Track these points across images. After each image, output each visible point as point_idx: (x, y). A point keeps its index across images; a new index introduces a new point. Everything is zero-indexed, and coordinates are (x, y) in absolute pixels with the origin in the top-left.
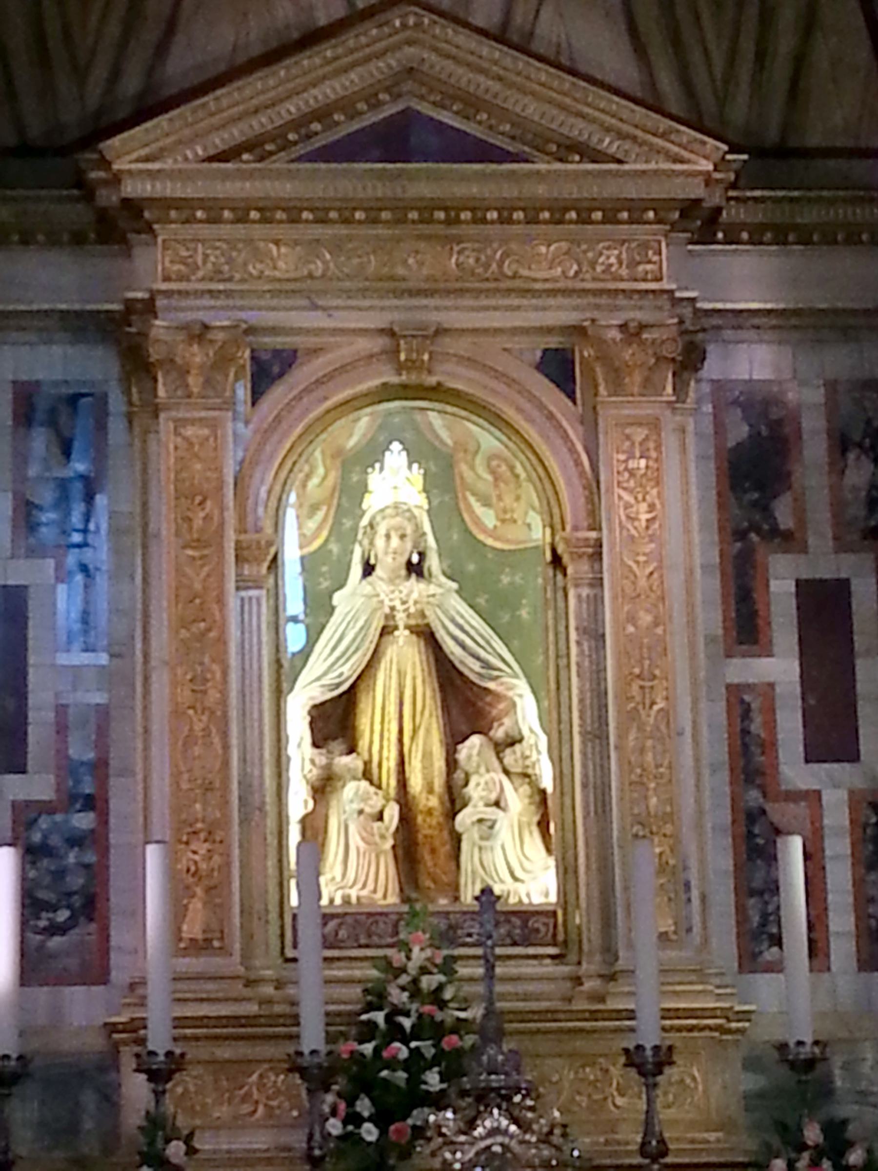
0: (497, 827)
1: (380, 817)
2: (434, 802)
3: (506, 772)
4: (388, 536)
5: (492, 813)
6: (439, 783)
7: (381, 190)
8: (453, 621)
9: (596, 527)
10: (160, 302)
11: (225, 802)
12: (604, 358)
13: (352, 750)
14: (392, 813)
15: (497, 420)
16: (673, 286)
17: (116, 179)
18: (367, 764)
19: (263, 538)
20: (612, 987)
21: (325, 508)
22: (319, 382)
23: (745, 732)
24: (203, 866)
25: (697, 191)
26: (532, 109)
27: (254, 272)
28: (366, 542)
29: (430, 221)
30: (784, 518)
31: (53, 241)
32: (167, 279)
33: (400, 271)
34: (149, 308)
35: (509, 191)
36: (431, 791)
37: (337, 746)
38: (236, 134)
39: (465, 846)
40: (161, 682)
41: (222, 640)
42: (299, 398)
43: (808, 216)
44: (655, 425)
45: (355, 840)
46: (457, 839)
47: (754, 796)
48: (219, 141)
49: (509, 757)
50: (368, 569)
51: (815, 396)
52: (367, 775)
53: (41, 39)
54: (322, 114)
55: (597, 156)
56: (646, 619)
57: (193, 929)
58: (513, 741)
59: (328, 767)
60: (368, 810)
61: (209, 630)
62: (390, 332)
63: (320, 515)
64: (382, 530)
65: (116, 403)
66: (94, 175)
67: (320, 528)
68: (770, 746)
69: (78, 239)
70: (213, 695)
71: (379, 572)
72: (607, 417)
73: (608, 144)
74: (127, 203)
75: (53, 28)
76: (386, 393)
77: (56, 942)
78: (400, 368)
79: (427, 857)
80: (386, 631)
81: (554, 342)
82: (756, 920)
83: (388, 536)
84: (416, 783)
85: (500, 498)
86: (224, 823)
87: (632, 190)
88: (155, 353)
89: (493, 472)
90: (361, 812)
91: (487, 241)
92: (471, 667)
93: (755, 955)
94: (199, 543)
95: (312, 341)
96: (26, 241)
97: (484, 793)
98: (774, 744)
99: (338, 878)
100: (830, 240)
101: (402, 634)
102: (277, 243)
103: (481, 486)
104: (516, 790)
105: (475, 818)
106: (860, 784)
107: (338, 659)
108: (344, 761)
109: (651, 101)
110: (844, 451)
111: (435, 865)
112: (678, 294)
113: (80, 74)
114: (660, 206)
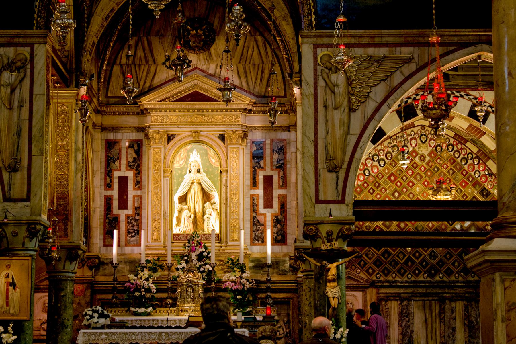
1: (190, 217)
2: (200, 214)
3: (213, 209)
5: (210, 216)
6: (201, 210)
7: (190, 107)
9: (227, 167)
10: (151, 127)
11: (160, 216)
12: (230, 137)
13: (186, 204)
14: (192, 216)
15: (211, 147)
18: (189, 207)
19: (168, 169)
20: (227, 248)
22: (179, 141)
23: (253, 203)
24: (157, 227)
25: (246, 107)
29: (199, 112)
30: (262, 164)
31: (133, 114)
32: (152, 122)
33: (194, 121)
34: (149, 127)
35: (213, 107)
36: (199, 212)
37: (184, 204)
38: (164, 97)
40: (150, 194)
41: (161, 187)
42: (176, 143)
45: (186, 221)
46: (204, 220)
47: (254, 214)
48: (161, 98)
49: (213, 206)
50: (190, 172)
51: (268, 142)
52: (188, 209)
54: (180, 92)
56: (235, 184)
57: (155, 237)
58: (214, 203)
59: (182, 207)
62: (191, 131)
64: (192, 164)
66: (140, 104)
67: (183, 163)
68: (257, 205)
69: (138, 113)
70: (159, 197)
71: (192, 172)
72: (230, 146)
74: (145, 109)
76: (191, 142)
77: (132, 239)
78: (194, 138)
80: (192, 183)
81: (221, 133)
82: (254, 236)
84: (197, 211)
86: (160, 219)
88: (150, 136)
91: (209, 115)
92: (207, 190)
93: (253, 243)
94: (158, 170)
98: (258, 205)
102: (172, 116)
106: (273, 212)
108: (185, 207)
109: (241, 87)
110: (273, 152)
114: (240, 109)
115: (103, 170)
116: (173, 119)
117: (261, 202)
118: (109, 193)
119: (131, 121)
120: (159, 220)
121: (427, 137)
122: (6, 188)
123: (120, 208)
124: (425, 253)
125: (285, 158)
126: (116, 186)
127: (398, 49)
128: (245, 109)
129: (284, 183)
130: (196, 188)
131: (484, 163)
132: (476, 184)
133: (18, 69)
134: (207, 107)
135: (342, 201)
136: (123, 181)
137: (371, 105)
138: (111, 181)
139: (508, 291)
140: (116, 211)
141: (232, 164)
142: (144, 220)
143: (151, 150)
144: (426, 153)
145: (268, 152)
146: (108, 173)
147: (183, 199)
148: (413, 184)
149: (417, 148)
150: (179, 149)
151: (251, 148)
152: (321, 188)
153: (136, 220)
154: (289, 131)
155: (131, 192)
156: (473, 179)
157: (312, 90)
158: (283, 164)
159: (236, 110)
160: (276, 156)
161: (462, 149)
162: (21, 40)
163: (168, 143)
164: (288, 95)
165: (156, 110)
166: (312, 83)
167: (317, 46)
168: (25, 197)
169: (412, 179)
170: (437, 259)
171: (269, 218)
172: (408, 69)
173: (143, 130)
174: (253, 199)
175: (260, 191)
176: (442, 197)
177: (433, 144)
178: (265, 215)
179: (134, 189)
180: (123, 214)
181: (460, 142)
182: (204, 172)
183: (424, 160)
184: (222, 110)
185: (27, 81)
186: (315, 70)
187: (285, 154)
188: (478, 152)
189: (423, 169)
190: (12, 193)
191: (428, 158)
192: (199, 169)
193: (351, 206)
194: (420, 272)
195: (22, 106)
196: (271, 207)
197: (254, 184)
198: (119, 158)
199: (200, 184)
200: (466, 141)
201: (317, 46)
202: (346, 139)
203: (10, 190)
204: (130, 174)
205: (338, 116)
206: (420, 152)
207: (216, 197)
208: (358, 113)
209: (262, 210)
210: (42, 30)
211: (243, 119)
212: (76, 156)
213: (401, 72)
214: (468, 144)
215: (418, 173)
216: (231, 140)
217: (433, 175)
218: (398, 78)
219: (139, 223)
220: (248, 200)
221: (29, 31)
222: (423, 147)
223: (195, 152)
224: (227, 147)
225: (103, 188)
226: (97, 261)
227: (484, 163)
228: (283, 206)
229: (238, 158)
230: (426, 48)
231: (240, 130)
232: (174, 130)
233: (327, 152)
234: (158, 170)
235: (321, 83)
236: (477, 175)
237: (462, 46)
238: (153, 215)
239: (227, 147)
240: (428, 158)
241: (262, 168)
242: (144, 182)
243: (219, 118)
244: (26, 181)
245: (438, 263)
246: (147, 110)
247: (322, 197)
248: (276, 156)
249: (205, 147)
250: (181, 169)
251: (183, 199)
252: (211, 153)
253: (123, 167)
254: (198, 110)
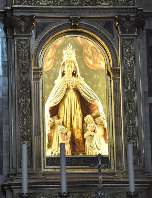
0: (94, 137)
1: (66, 134)
2: (79, 131)
3: (96, 124)
4: (68, 67)
5: (93, 133)
6: (80, 126)
8: (83, 87)
11: (31, 131)
13: (59, 118)
14: (69, 133)
16: (137, 7)
21: (52, 59)
27: (37, 3)
28: (62, 68)
37: (56, 117)
39: (86, 141)
46: (84, 140)
49: (97, 120)
50: (63, 75)
52: (63, 124)
58: (98, 116)
59: (54, 122)
60: (63, 132)
61: (26, 90)
63: (51, 61)
64: (66, 65)
71: (65, 75)
79: (77, 144)
80: (68, 90)
81: (108, 20)
83: (68, 67)
84: (75, 126)
85: (94, 57)
86: (31, 136)
89: (92, 51)
90: (62, 133)
92: (87, 98)
95: (50, 20)
97: (91, 129)
99: (57, 149)
101: (71, 91)
103: (89, 54)
104: (98, 128)
105: (89, 135)
107: (56, 97)
111: (79, 145)
112: (138, 9)
130: (72, 96)
147: (55, 111)
192: (76, 71)
199: (77, 91)
223: (70, 47)
251: (55, 111)
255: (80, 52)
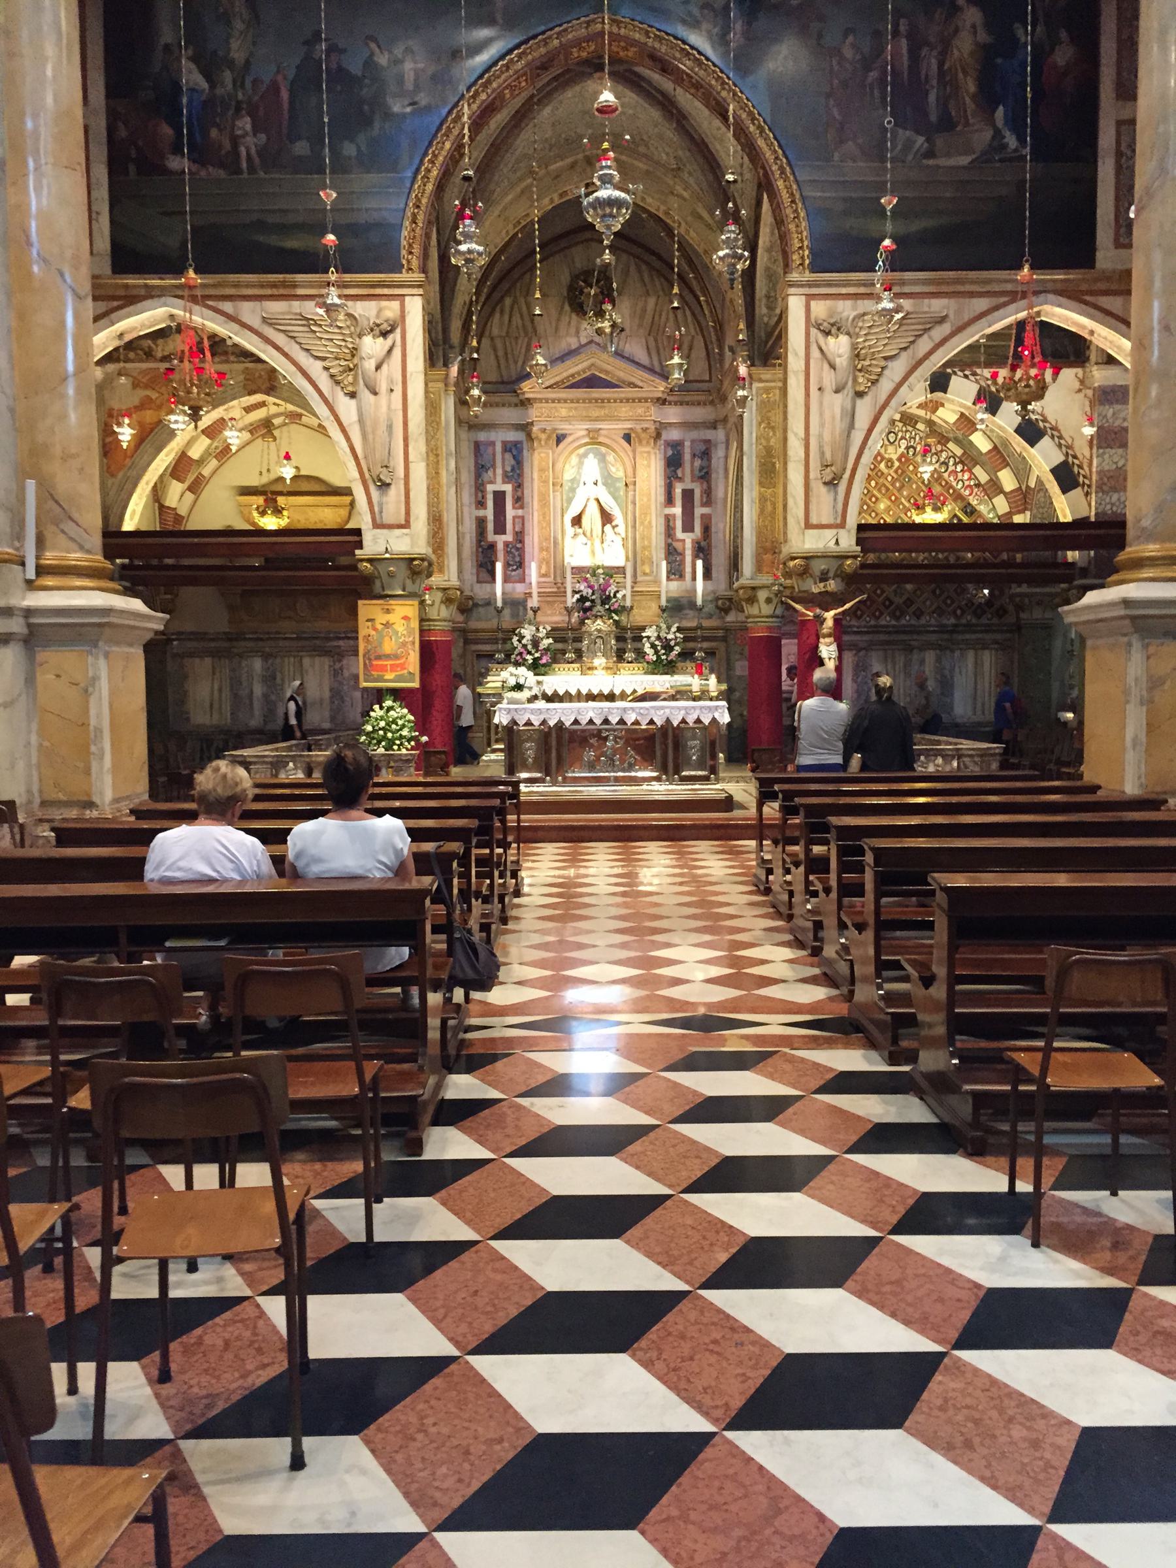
7: (586, 396)
12: (638, 436)
17: (524, 393)
25: (660, 395)
26: (621, 374)
30: (680, 475)
31: (510, 405)
34: (532, 424)
35: (616, 395)
38: (552, 381)
40: (536, 514)
43: (687, 399)
44: (649, 453)
48: (547, 384)
51: (687, 444)
52: (584, 534)
53: (506, 354)
54: (573, 376)
55: (636, 386)
57: (543, 571)
65: (525, 446)
68: (674, 529)
69: (516, 405)
73: (640, 384)
75: (509, 351)
87: (644, 395)
88: (533, 436)
96: (503, 405)
100: (693, 404)
108: (580, 531)
113: (516, 362)
114: (652, 399)
115: (473, 483)
116: (564, 412)
117: (679, 524)
118: (481, 513)
119: (509, 415)
120: (547, 549)
121: (896, 435)
122: (376, 509)
123: (496, 533)
124: (890, 590)
125: (709, 466)
126: (490, 503)
127: (926, 301)
128: (658, 399)
129: (708, 501)
131: (970, 471)
132: (958, 497)
133: (384, 334)
134: (607, 395)
135: (842, 525)
136: (499, 497)
137: (886, 386)
138: (483, 497)
139: (1151, 660)
140: (491, 537)
141: (642, 473)
142: (528, 549)
143: (536, 456)
144: (894, 457)
145: (687, 457)
146: (479, 488)
147: (577, 521)
148: (877, 499)
149: (882, 451)
150: (572, 452)
151: (665, 452)
152: (813, 507)
153: (518, 549)
154: (715, 428)
155: (510, 512)
156: (954, 490)
157: (802, 363)
158: (707, 473)
159: (646, 400)
160: (698, 463)
161: (942, 451)
162: (386, 291)
163: (557, 445)
164: (714, 378)
165: (540, 400)
166: (802, 353)
167: (810, 297)
168: (403, 522)
169: (875, 492)
170: (905, 598)
171: (689, 545)
172: (939, 333)
173: (526, 428)
174: (669, 519)
175: (677, 510)
176: (930, 517)
177: (904, 444)
178: (684, 541)
179: (514, 508)
180: (500, 540)
181: (939, 442)
182: (604, 484)
183: (892, 466)
184: (628, 400)
185: (397, 352)
186: (808, 334)
187: (709, 460)
188: (963, 455)
189: (889, 478)
190: (384, 515)
191: (897, 464)
193: (854, 532)
194: (881, 614)
195: (392, 390)
196: (692, 530)
197: (670, 501)
198: (494, 466)
199: (598, 500)
200: (948, 440)
201: (810, 297)
202: (848, 436)
203: (381, 512)
204: (508, 488)
205: (837, 403)
206: (887, 456)
207: (619, 519)
208: (867, 399)
209: (680, 534)
210: (415, 275)
211: (654, 413)
212: (447, 464)
213: (930, 337)
214: (951, 445)
215: (884, 485)
216: (640, 441)
217: (902, 487)
218: (924, 345)
219: (521, 551)
220: (662, 520)
221: (396, 277)
222: (891, 449)
223: (591, 456)
224: (634, 451)
225: (474, 506)
226: (471, 603)
227: (970, 471)
228: (706, 530)
229: (649, 466)
230: (967, 300)
231: (652, 427)
232: (564, 427)
233: (822, 454)
234: (546, 482)
235: (815, 353)
236: (959, 486)
237: (1014, 296)
238: (540, 543)
239: (634, 451)
240: (897, 464)
241: (680, 479)
242: (527, 499)
243: (624, 410)
244: (403, 498)
245: (904, 602)
246: (528, 400)
247: (814, 520)
248: (698, 463)
249: (603, 449)
250: (573, 481)
251: (577, 521)
252: (611, 458)
253: (499, 479)
254: (596, 400)
255: (602, 459)
